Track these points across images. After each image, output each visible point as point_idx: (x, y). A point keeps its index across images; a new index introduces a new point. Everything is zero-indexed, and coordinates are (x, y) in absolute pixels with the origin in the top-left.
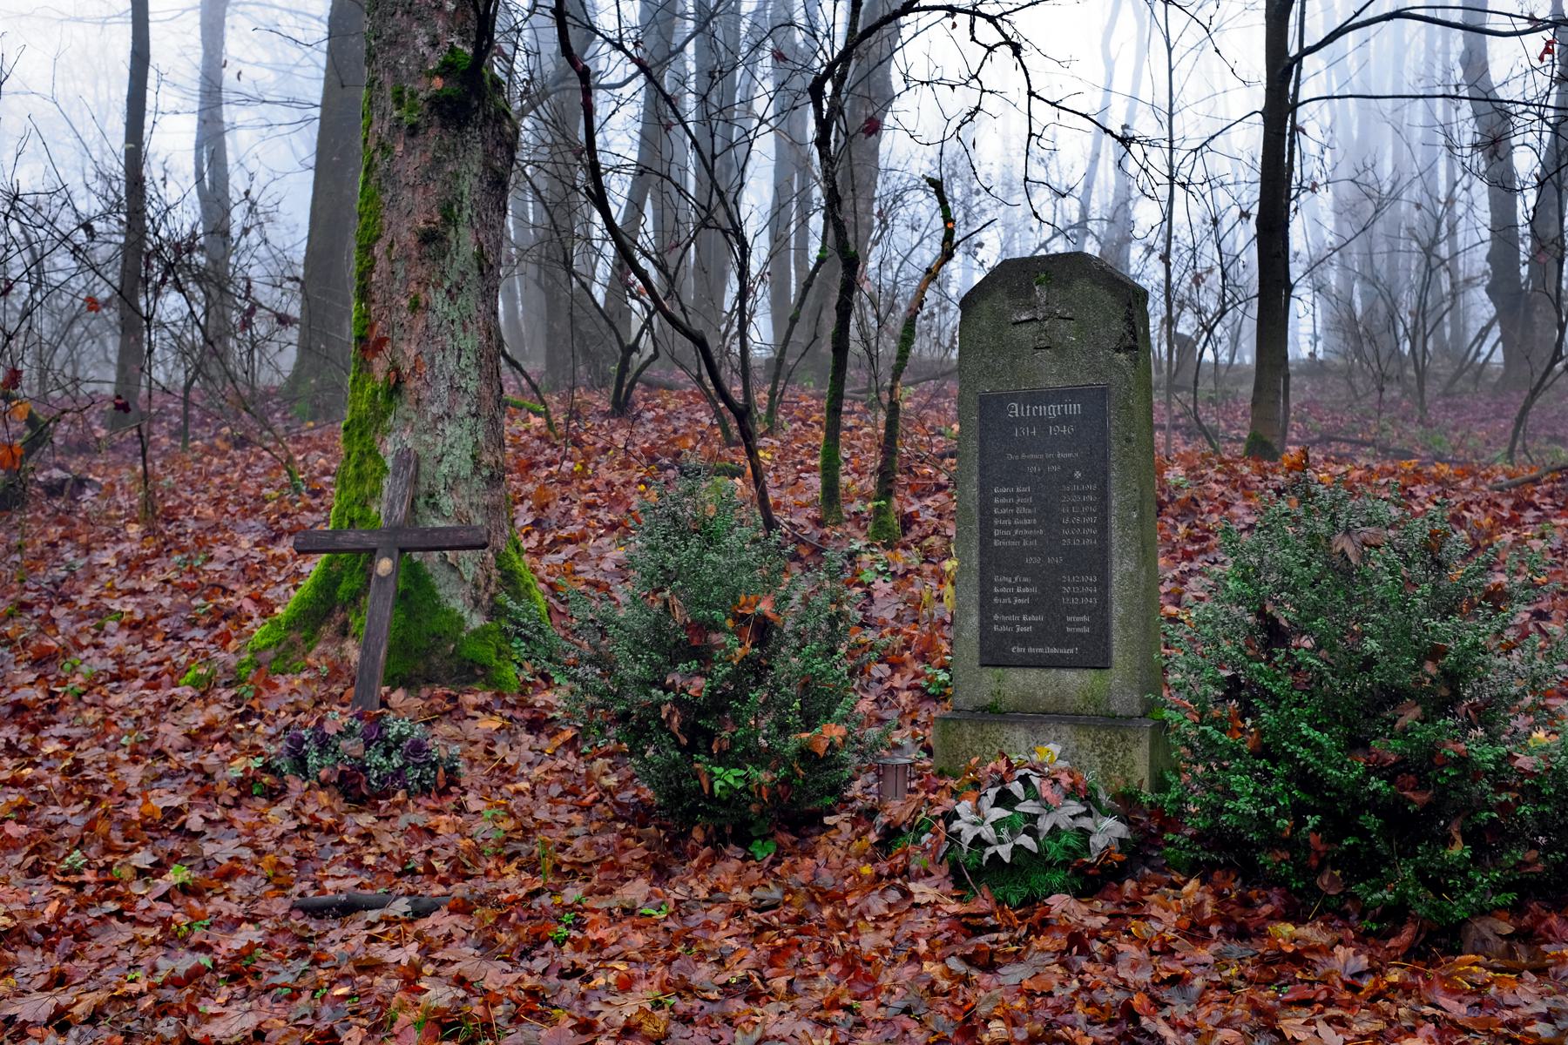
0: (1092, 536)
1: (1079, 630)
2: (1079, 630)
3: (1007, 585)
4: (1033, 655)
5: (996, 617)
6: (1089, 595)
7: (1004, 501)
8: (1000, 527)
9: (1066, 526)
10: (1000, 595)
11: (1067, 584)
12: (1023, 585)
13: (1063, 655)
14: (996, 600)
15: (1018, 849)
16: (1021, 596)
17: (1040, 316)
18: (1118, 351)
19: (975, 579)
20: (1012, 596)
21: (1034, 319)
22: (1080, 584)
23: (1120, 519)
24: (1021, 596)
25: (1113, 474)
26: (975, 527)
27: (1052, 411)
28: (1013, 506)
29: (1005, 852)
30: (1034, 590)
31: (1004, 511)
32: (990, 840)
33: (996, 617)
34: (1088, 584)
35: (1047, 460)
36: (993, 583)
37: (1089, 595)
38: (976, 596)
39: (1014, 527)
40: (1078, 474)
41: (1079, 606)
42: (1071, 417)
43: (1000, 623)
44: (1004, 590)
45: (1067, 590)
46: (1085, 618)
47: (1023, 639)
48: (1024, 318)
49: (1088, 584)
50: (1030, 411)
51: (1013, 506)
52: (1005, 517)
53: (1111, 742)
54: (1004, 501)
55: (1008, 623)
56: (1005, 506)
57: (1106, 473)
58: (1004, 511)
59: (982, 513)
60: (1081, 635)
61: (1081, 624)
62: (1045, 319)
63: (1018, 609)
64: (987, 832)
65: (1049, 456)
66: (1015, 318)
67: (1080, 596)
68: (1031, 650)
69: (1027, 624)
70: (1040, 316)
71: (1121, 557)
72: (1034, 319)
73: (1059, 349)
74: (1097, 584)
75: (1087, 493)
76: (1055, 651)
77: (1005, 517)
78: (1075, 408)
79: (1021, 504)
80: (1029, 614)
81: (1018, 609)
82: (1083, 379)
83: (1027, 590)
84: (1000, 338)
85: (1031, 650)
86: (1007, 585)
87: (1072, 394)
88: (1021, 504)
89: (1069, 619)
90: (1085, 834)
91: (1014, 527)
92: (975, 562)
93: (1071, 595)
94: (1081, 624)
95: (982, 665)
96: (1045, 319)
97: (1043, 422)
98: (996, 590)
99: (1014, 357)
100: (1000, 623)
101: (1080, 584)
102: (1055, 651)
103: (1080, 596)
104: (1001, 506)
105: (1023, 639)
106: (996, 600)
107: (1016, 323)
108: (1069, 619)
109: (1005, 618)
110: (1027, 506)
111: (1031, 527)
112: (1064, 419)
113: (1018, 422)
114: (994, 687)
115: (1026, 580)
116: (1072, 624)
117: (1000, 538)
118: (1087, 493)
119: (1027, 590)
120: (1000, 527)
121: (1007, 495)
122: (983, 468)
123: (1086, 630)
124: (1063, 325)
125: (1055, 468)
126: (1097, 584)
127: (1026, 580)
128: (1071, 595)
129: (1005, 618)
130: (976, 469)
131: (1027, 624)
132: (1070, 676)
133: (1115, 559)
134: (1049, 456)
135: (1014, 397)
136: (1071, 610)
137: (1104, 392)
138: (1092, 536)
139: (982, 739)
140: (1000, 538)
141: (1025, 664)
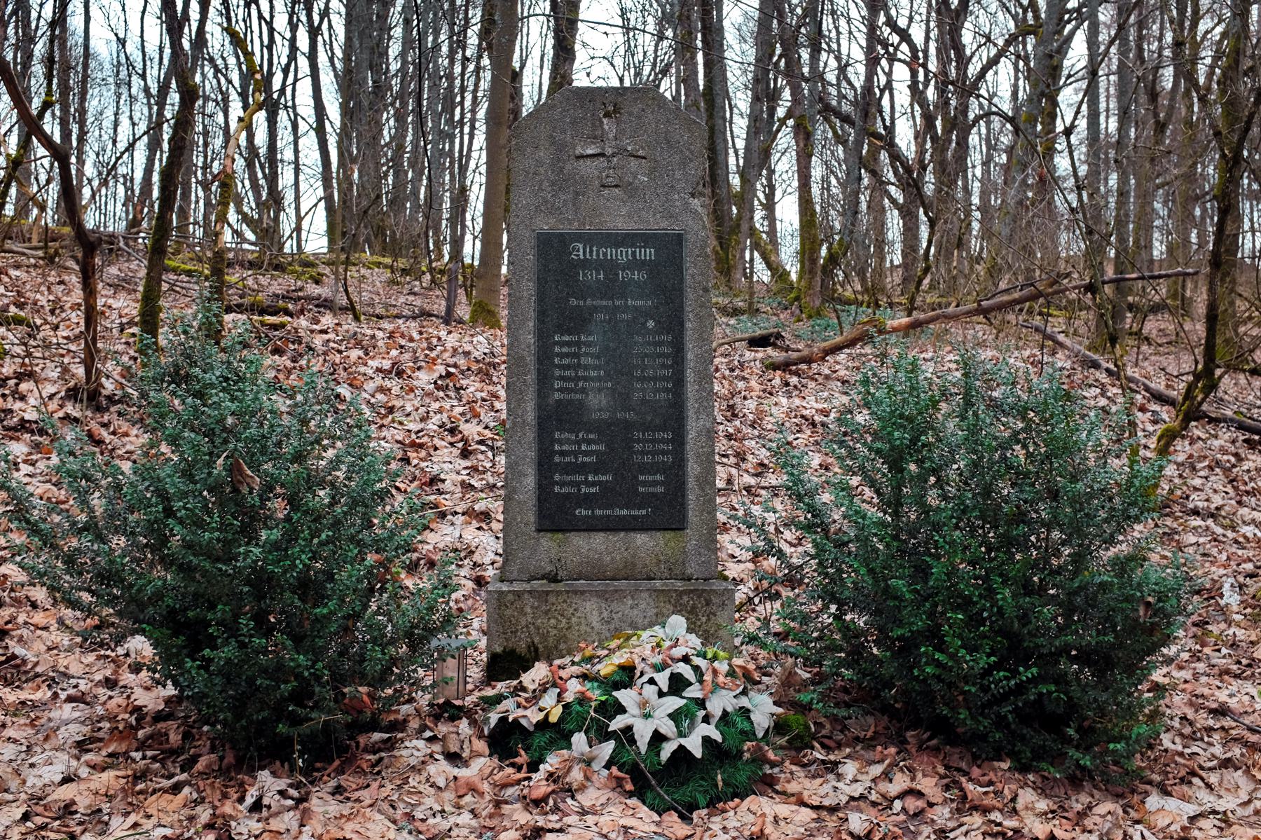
0: (667, 390)
1: (652, 489)
2: (652, 489)
3: (569, 441)
4: (602, 517)
5: (557, 477)
6: (663, 453)
7: (565, 350)
8: (562, 378)
9: (639, 379)
10: (562, 453)
11: (638, 441)
12: (589, 442)
13: (635, 518)
14: (557, 459)
15: (707, 741)
16: (586, 453)
17: (609, 151)
18: (693, 195)
19: (531, 435)
20: (576, 454)
21: (602, 155)
22: (654, 441)
23: (697, 372)
24: (586, 453)
25: (689, 325)
26: (531, 378)
27: (622, 255)
28: (576, 355)
29: (694, 744)
30: (602, 447)
31: (567, 361)
32: (670, 735)
33: (557, 477)
34: (663, 441)
35: (616, 308)
36: (553, 441)
37: (663, 453)
38: (532, 454)
39: (578, 378)
40: (651, 324)
41: (652, 464)
42: (643, 262)
43: (562, 484)
44: (566, 447)
45: (638, 447)
46: (659, 477)
47: (588, 501)
48: (590, 152)
49: (663, 441)
50: (596, 253)
51: (576, 355)
52: (568, 367)
53: (694, 607)
54: (565, 350)
55: (571, 484)
56: (567, 355)
57: (682, 324)
58: (567, 361)
59: (540, 361)
60: (654, 495)
61: (655, 484)
62: (613, 155)
63: (582, 469)
64: (668, 728)
65: (618, 303)
66: (579, 151)
67: (653, 453)
68: (597, 512)
69: (593, 484)
70: (609, 151)
71: (697, 412)
72: (602, 155)
73: (631, 190)
74: (672, 441)
75: (661, 344)
76: (625, 512)
77: (568, 367)
78: (649, 253)
79: (587, 354)
80: (596, 473)
81: (582, 469)
82: (656, 223)
83: (593, 447)
84: (562, 169)
85: (597, 512)
86: (569, 441)
87: (645, 239)
88: (587, 354)
89: (641, 478)
90: (745, 712)
91: (578, 378)
92: (531, 416)
93: (643, 453)
94: (655, 484)
95: (539, 531)
96: (613, 155)
97: (610, 267)
98: (557, 447)
99: (577, 194)
100: (562, 484)
101: (654, 441)
102: (625, 512)
103: (653, 453)
104: (562, 356)
105: (588, 501)
106: (557, 459)
107: (582, 157)
108: (641, 478)
109: (567, 478)
110: (592, 356)
111: (599, 379)
112: (635, 264)
113: (584, 264)
114: (553, 554)
115: (591, 436)
116: (644, 483)
117: (561, 390)
118: (661, 344)
119: (593, 447)
120: (562, 378)
121: (568, 344)
122: (542, 315)
123: (660, 489)
124: (634, 163)
125: (625, 316)
126: (672, 441)
127: (591, 436)
128: (643, 453)
129: (567, 478)
130: (532, 314)
131: (593, 484)
132: (641, 539)
133: (691, 413)
134: (618, 303)
135: (579, 237)
136: (643, 469)
137: (679, 239)
138: (667, 390)
139: (546, 613)
140: (561, 390)
141: (591, 527)
